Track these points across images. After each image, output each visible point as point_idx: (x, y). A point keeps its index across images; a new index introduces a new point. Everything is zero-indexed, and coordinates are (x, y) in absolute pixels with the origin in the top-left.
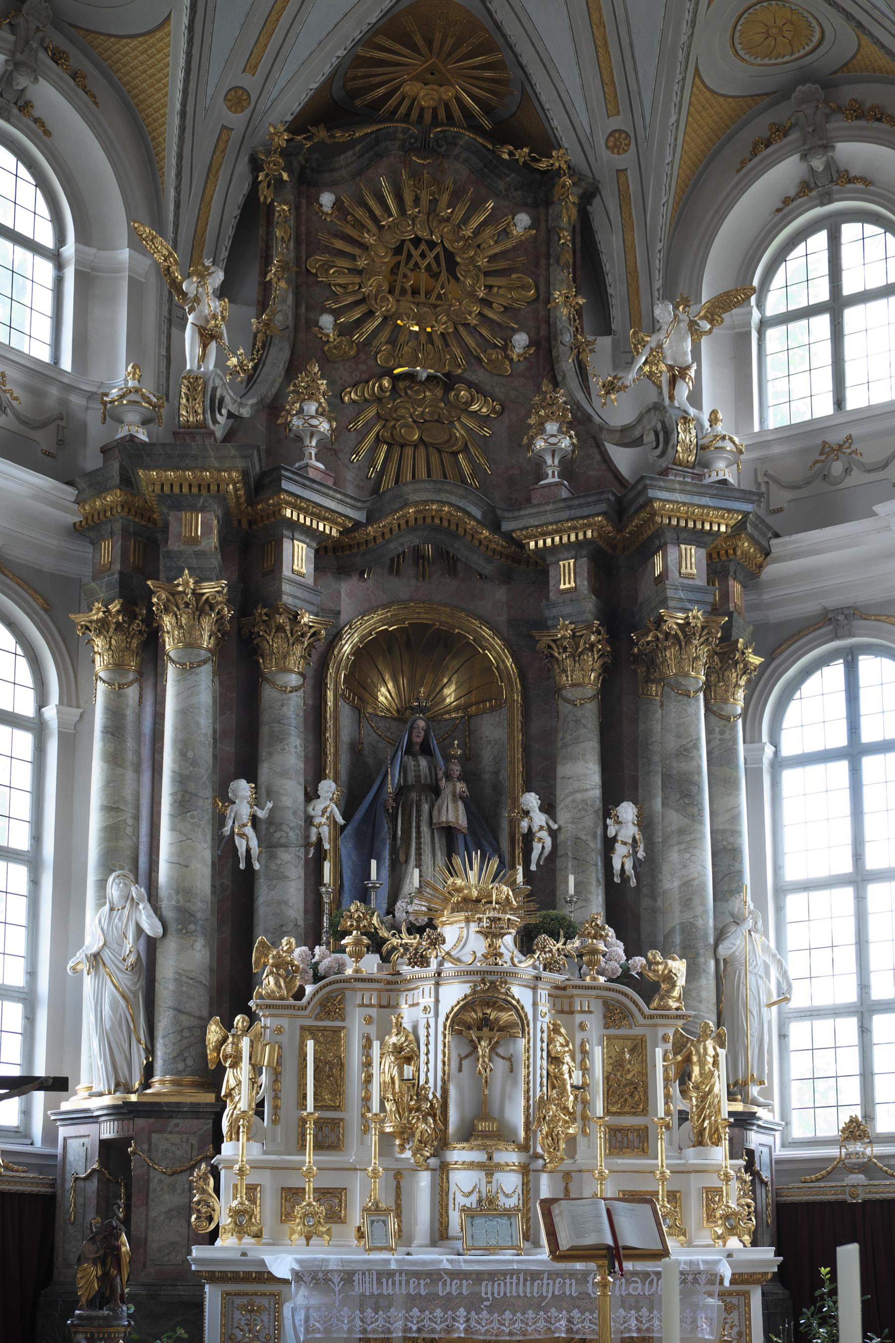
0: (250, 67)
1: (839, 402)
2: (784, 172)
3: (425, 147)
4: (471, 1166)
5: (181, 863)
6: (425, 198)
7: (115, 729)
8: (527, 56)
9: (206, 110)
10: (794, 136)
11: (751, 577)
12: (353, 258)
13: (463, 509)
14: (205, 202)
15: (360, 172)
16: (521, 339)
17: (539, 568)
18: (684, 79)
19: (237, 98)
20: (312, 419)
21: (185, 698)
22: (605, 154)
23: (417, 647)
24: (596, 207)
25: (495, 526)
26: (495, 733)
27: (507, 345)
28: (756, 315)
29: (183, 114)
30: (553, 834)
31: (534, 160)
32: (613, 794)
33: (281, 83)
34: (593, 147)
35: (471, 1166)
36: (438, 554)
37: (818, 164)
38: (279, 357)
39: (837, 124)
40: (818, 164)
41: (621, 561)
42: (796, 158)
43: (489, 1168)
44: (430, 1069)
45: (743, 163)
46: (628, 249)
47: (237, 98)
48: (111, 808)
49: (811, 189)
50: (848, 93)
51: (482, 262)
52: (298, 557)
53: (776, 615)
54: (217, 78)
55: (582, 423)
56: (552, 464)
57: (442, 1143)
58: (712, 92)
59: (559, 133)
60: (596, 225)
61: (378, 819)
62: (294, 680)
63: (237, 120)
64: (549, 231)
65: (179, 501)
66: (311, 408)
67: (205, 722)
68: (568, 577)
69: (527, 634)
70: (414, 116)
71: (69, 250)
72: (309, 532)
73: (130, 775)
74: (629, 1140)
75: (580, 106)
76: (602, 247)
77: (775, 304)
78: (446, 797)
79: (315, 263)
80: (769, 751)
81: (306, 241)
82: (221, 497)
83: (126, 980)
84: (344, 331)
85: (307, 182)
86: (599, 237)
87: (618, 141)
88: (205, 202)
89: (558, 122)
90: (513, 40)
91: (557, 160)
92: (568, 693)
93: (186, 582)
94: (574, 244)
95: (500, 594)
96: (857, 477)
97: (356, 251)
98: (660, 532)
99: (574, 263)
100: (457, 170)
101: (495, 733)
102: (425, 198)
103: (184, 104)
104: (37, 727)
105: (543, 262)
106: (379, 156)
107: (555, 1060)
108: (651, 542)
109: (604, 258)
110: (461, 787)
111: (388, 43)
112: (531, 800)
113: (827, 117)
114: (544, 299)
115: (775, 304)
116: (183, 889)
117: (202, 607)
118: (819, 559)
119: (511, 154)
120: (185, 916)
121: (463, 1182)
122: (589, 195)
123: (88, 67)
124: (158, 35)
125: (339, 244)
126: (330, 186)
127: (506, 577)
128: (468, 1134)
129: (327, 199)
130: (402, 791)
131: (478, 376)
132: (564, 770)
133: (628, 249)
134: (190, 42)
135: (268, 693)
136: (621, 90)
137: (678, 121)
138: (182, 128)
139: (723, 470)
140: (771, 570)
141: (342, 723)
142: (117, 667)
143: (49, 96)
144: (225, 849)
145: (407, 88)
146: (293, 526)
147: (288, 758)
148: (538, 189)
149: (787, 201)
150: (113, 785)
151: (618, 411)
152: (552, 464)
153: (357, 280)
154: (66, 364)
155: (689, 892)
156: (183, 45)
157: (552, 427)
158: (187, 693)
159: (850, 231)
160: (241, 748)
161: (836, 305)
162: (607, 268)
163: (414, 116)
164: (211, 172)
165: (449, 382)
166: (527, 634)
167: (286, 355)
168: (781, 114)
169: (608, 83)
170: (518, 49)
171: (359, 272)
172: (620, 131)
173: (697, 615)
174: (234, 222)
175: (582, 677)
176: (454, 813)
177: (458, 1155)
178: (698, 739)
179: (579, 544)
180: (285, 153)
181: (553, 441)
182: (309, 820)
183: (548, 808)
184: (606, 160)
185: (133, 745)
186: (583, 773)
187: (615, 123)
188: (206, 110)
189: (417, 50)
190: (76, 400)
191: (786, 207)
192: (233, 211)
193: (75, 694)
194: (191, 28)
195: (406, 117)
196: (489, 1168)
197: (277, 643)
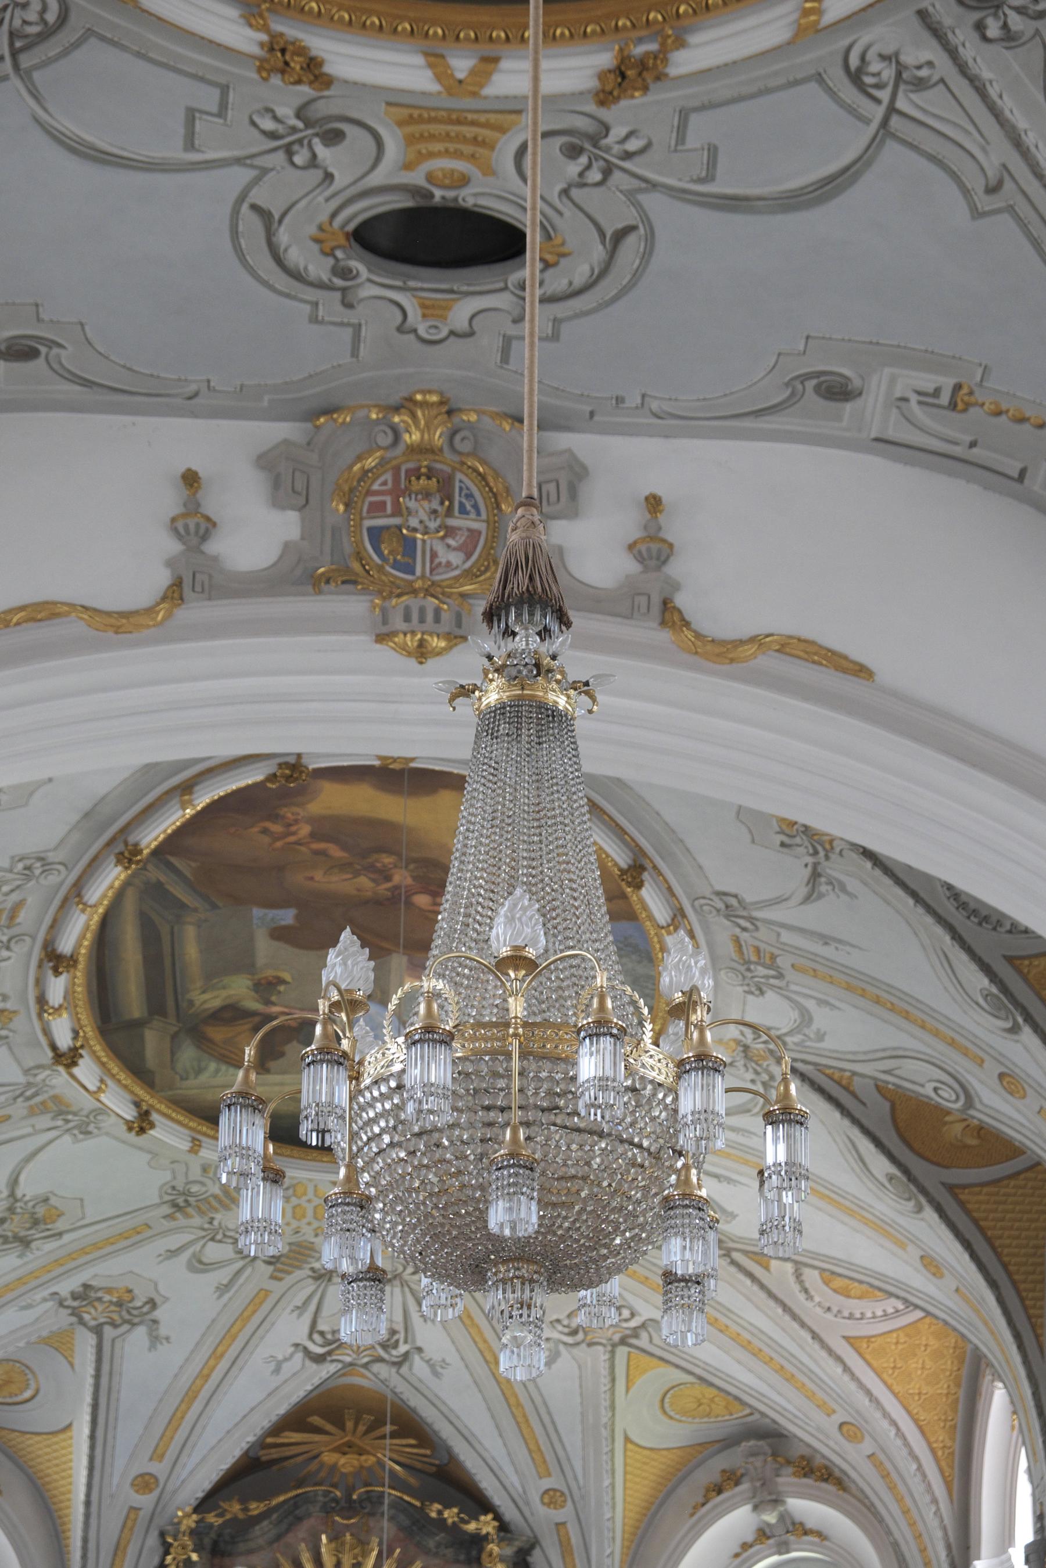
0: (157, 1455)
2: (737, 1520)
10: (745, 1486)
15: (278, 1538)
29: (88, 1503)
39: (786, 1480)
45: (696, 1508)
47: (145, 1483)
54: (122, 1468)
58: (651, 1449)
63: (146, 1501)
87: (553, 1498)
89: (487, 1484)
124: (62, 1436)
137: (613, 1485)
138: (87, 1516)
149: (745, 1546)
180: (192, 1532)
184: (543, 1517)
187: (547, 1483)
189: (327, 1433)
194: (92, 1437)
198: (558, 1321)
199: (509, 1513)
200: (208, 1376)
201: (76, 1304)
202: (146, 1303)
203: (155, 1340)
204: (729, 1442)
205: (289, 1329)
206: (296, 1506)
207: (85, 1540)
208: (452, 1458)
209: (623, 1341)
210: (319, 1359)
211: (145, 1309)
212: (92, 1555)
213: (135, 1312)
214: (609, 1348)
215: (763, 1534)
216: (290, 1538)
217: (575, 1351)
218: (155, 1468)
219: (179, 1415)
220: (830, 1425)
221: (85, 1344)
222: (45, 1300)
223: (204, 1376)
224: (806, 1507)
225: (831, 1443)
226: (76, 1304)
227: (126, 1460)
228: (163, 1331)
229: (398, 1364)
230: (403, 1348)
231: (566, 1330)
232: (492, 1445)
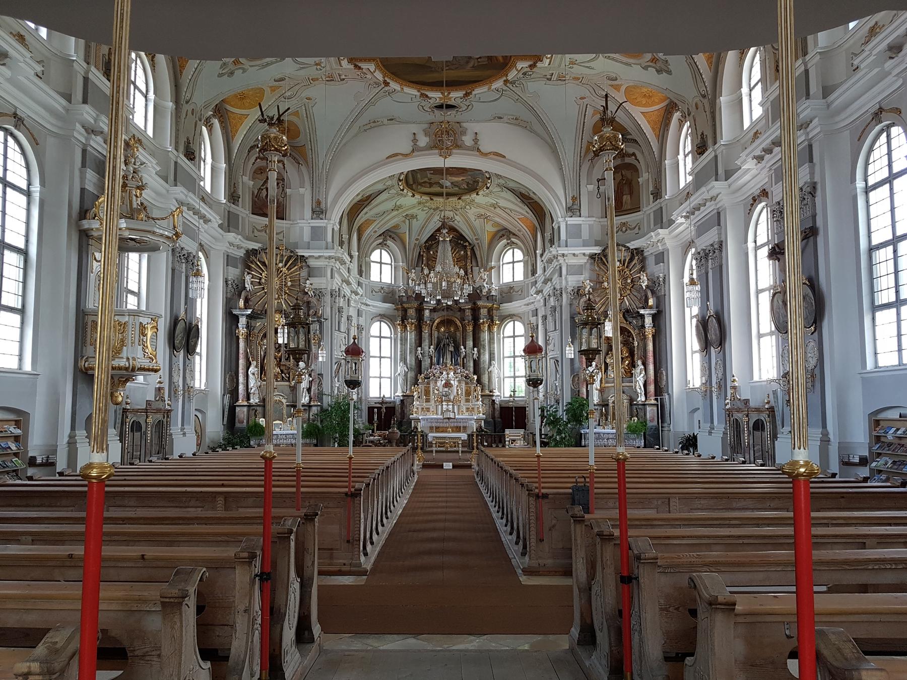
2: (504, 241)
7: (401, 340)
11: (498, 309)
17: (464, 310)
21: (411, 336)
32: (474, 347)
41: (475, 311)
47: (417, 240)
54: (413, 239)
61: (440, 349)
69: (462, 320)
74: (467, 401)
101: (459, 335)
104: (391, 338)
108: (479, 309)
118: (508, 307)
141: (435, 334)
143: (389, 243)
144: (417, 357)
147: (426, 343)
150: (401, 348)
160: (419, 343)
166: (462, 320)
175: (470, 329)
176: (452, 349)
185: (404, 340)
186: (470, 343)
191: (505, 246)
193: (396, 333)
205: (437, 218)
227: (414, 236)
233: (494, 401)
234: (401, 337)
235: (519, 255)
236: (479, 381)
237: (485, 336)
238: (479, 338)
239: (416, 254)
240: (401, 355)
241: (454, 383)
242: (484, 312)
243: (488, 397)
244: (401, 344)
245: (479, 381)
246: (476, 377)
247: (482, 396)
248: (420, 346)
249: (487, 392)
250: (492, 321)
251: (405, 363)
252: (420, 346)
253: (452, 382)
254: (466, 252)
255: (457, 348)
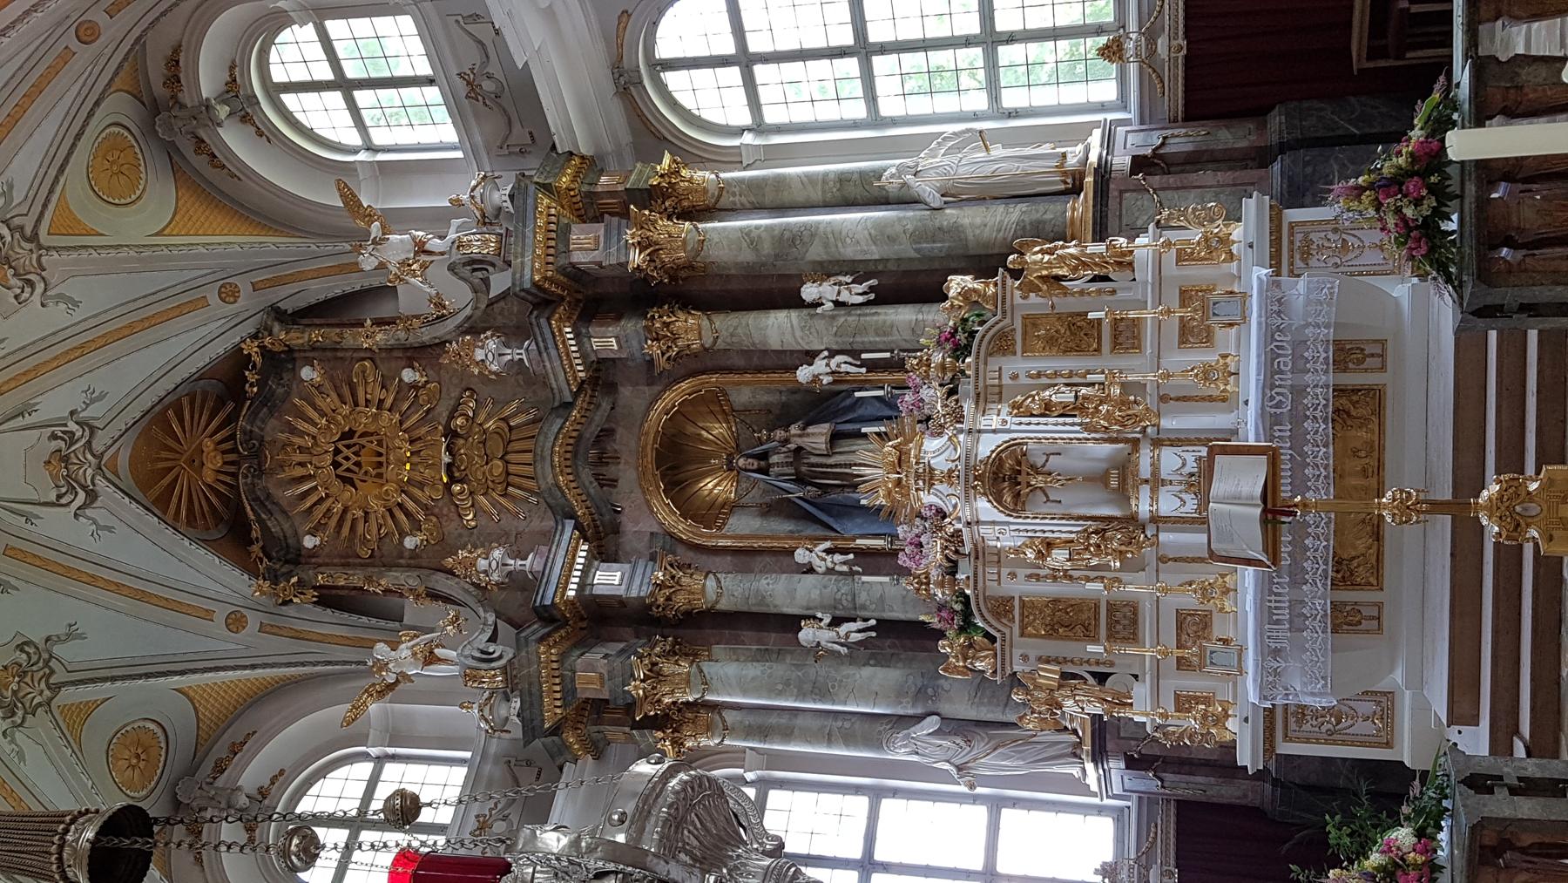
0: (208, 615)
1: (430, 81)
2: (234, 140)
3: (257, 454)
4: (1154, 498)
5: (875, 697)
6: (299, 458)
7: (763, 733)
8: (168, 384)
9: (248, 647)
10: (202, 134)
11: (592, 165)
12: (354, 520)
13: (555, 436)
14: (323, 639)
15: (284, 512)
16: (408, 375)
18: (167, 246)
19: (235, 622)
20: (493, 562)
21: (731, 679)
22: (241, 302)
23: (675, 463)
24: (288, 306)
25: (568, 406)
26: (744, 393)
27: (414, 386)
28: (363, 156)
29: (253, 667)
30: (833, 353)
31: (254, 366)
33: (221, 589)
34: (237, 315)
35: (1154, 498)
36: (596, 452)
37: (222, 111)
38: (442, 583)
39: (185, 97)
40: (222, 111)
42: (220, 130)
43: (1156, 482)
44: (1063, 530)
45: (233, 176)
46: (320, 274)
47: (235, 622)
48: (829, 740)
49: (246, 114)
50: (159, 90)
51: (346, 409)
52: (609, 579)
53: (625, 138)
55: (474, 328)
56: (511, 354)
57: (1133, 519)
59: (229, 345)
60: (303, 304)
61: (823, 502)
62: (711, 583)
63: (253, 620)
64: (314, 349)
65: (569, 692)
66: (482, 564)
67: (753, 670)
68: (606, 341)
69: (655, 376)
70: (232, 469)
71: (374, 751)
72: (586, 571)
73: (800, 721)
74: (1126, 336)
75: (203, 331)
76: (322, 298)
77: (352, 138)
78: (805, 442)
79: (365, 553)
80: (748, 138)
81: (347, 560)
82: (563, 657)
83: (979, 746)
84: (417, 527)
85: (296, 557)
86: (313, 301)
87: (228, 294)
88: (323, 639)
89: (220, 348)
90: (156, 399)
91: (252, 348)
92: (708, 342)
93: (636, 689)
94: (321, 326)
95: (626, 392)
96: (494, 68)
97: (349, 517)
98: (562, 270)
99: (338, 325)
100: (272, 429)
101: (744, 393)
102: (299, 458)
103: (245, 667)
105: (340, 354)
106: (269, 496)
107: (1048, 409)
109: (330, 295)
110: (794, 429)
111: (175, 500)
112: (804, 374)
113: (183, 106)
114: (371, 355)
115: (352, 138)
116: (899, 695)
117: (655, 674)
118: (571, 106)
119: (252, 385)
120: (920, 694)
121: (1168, 505)
122: (278, 314)
123: (227, 738)
124: (192, 693)
125: (346, 531)
126: (299, 542)
127: (611, 388)
128: (1122, 495)
129: (309, 542)
130: (800, 480)
131: (443, 412)
132: (774, 343)
133: (320, 274)
134: (194, 671)
135: (723, 605)
136: (184, 298)
137: (204, 245)
138: (265, 666)
139: (500, 196)
140: (584, 151)
141: (743, 527)
142: (709, 729)
144: (862, 653)
145: (209, 480)
146: (582, 586)
147: (779, 591)
148: (280, 362)
150: (808, 737)
151: (459, 296)
152: (511, 354)
153: (372, 516)
154: (468, 755)
155: (881, 234)
156: (197, 676)
157: (479, 355)
158: (728, 688)
159: (278, 75)
161: (344, 85)
162: (339, 292)
163: (232, 469)
164: (298, 636)
165: (451, 434)
167: (440, 576)
168: (187, 147)
169: (180, 311)
170: (163, 394)
171: (366, 513)
172: (220, 293)
173: (630, 235)
174: (337, 613)
175: (693, 329)
176: (817, 437)
177: (1143, 506)
178: (741, 229)
179: (577, 336)
180: (275, 581)
181: (490, 353)
182: (830, 571)
183: (810, 356)
184: (248, 302)
186: (777, 328)
187: (214, 299)
188: (248, 647)
190: (494, 747)
191: (266, 133)
192: (328, 614)
194: (182, 673)
195: (234, 475)
196: (1156, 482)
197: (681, 600)
198: (16, 297)
199: (249, 327)
200: (117, 584)
201: (20, 713)
202: (22, 651)
203: (71, 635)
204: (171, 152)
206: (257, 499)
207: (289, 665)
208: (202, 376)
209: (34, 238)
210: (92, 496)
211: (31, 651)
212: (293, 659)
213: (35, 658)
214: (43, 252)
215: (246, 119)
216: (284, 503)
217: (53, 281)
218: (220, 617)
219: (163, 603)
220: (84, 53)
221: (68, 696)
222: (13, 741)
223: (118, 588)
224: (208, 82)
225: (108, 52)
226: (20, 713)
228: (62, 631)
229: (93, 429)
230: (72, 426)
231: (28, 290)
232: (177, 346)
233: (1139, 164)
234: (749, 732)
235: (294, 53)
236: (985, 263)
237: (728, 236)
238: (751, 273)
239: (330, 623)
240: (849, 739)
241: (994, 429)
242: (588, 246)
243: (1107, 197)
244: (787, 734)
245: (985, 263)
246: (957, 284)
247: (1100, 234)
248: (791, 623)
249: (1080, 208)
250: (648, 197)
251: (904, 722)
252: (791, 623)
253: (987, 447)
254: (313, 353)
255: (825, 404)
